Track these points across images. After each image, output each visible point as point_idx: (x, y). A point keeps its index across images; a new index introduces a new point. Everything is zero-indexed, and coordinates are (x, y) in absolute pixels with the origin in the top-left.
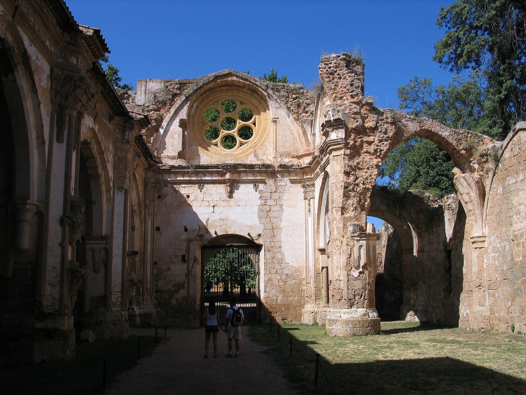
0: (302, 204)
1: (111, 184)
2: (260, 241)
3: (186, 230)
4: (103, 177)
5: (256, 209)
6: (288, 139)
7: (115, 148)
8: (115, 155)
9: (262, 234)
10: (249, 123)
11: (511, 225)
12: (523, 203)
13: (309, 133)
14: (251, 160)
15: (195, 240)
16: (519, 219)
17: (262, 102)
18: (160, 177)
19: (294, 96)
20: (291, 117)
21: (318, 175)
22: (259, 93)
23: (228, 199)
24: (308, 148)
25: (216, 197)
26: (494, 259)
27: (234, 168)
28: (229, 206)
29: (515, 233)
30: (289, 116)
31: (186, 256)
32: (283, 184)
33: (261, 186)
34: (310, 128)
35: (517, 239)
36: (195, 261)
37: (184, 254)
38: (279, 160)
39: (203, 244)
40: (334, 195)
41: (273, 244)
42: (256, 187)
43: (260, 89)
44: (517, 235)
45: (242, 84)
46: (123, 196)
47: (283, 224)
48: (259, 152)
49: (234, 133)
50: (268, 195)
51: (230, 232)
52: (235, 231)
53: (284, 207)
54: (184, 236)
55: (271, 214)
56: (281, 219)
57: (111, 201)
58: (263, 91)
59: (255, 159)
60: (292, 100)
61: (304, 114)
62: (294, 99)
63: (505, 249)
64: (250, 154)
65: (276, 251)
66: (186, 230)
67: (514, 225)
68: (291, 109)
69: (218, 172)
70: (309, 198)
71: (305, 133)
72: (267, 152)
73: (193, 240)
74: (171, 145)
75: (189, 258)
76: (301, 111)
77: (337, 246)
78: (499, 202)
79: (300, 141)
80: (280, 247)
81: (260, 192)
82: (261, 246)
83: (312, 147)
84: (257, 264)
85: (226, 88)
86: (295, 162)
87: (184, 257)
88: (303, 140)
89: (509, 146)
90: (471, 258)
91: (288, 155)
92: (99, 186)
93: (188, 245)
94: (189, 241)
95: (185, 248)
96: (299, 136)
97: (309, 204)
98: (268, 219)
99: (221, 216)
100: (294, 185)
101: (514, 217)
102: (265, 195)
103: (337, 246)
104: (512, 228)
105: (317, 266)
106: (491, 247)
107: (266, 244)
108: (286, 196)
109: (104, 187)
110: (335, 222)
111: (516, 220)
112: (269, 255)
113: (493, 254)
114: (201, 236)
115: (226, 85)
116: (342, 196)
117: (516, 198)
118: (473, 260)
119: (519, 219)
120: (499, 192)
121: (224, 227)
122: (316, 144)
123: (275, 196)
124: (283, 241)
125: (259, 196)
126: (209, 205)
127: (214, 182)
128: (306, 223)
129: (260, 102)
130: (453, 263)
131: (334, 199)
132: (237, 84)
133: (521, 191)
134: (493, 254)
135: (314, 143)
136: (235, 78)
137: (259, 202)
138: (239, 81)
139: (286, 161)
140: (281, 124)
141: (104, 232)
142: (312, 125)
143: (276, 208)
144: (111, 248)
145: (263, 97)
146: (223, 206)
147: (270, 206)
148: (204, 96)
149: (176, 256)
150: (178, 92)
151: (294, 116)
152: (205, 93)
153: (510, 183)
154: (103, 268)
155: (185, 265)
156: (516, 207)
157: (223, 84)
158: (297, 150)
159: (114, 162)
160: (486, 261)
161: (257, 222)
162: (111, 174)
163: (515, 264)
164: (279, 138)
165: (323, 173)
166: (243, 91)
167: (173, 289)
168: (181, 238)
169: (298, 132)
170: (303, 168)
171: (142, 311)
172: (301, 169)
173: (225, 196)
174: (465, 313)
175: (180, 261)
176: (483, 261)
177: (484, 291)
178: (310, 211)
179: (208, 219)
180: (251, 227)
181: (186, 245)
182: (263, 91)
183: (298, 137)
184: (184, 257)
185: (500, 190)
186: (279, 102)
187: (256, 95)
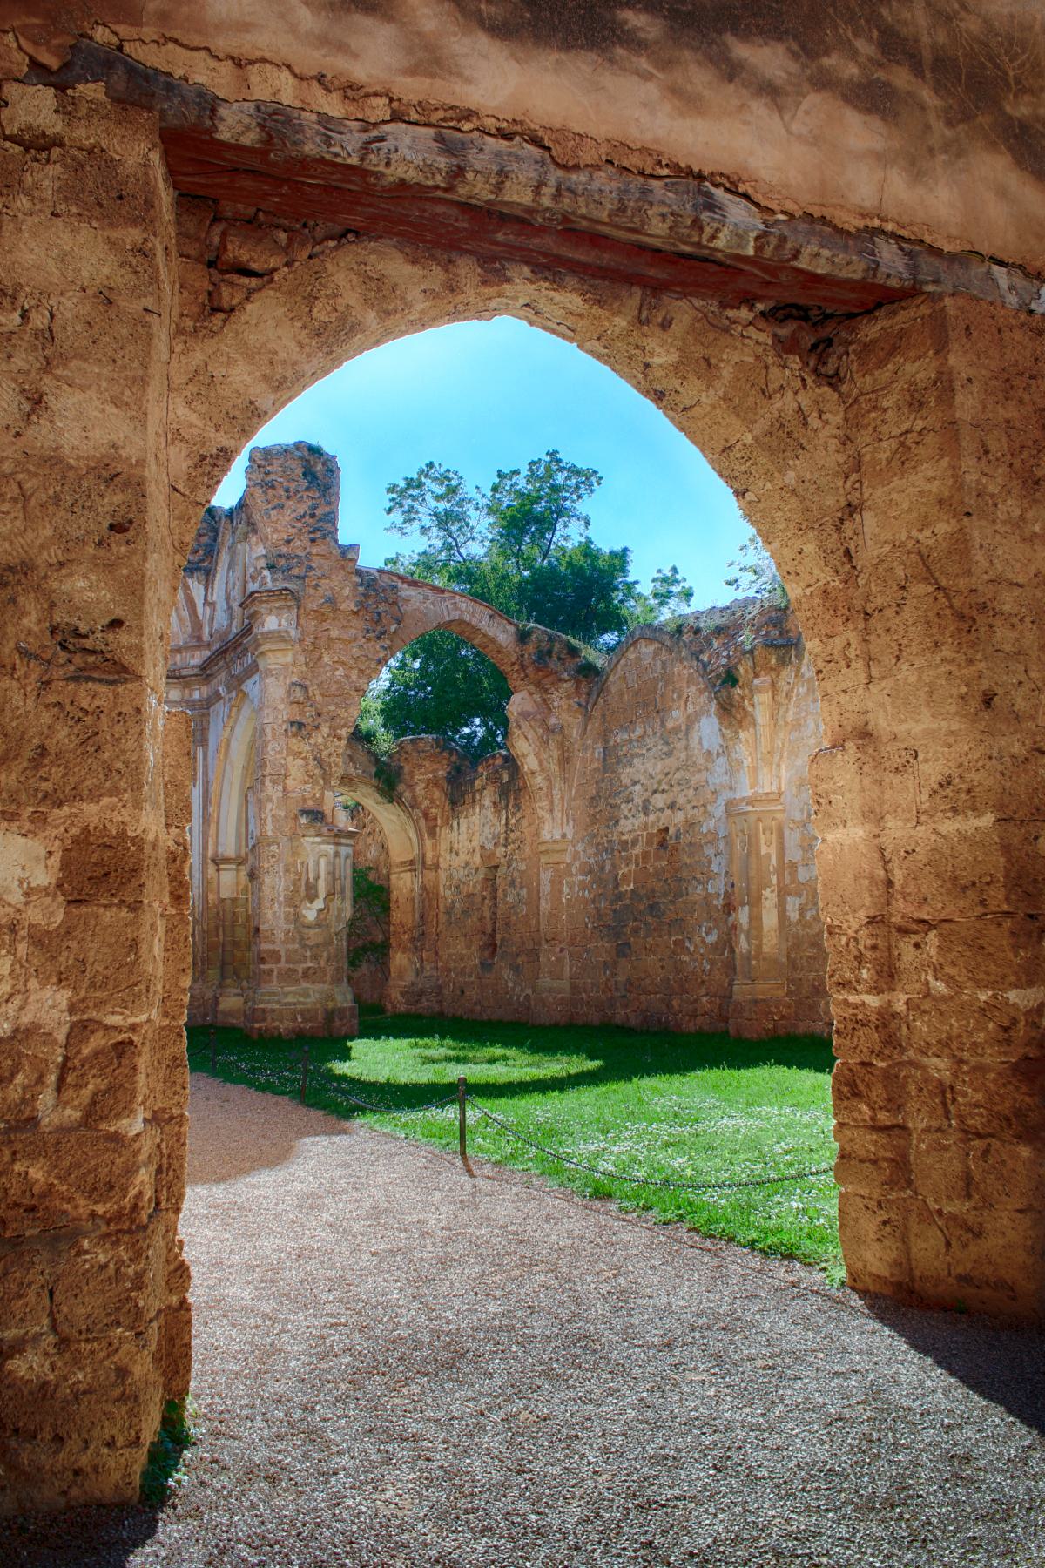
11: (617, 822)
13: (199, 602)
16: (630, 810)
26: (583, 887)
29: (624, 838)
34: (202, 587)
35: (625, 850)
44: (626, 842)
63: (602, 869)
67: (622, 822)
77: (273, 856)
83: (206, 630)
89: (619, 667)
90: (538, 885)
101: (623, 806)
104: (619, 828)
105: (211, 897)
106: (577, 864)
110: (269, 806)
111: (626, 813)
113: (581, 878)
118: (542, 887)
122: (216, 626)
130: (500, 893)
134: (581, 878)
156: (627, 787)
160: (566, 890)
163: (620, 896)
174: (523, 994)
176: (561, 892)
177: (562, 950)
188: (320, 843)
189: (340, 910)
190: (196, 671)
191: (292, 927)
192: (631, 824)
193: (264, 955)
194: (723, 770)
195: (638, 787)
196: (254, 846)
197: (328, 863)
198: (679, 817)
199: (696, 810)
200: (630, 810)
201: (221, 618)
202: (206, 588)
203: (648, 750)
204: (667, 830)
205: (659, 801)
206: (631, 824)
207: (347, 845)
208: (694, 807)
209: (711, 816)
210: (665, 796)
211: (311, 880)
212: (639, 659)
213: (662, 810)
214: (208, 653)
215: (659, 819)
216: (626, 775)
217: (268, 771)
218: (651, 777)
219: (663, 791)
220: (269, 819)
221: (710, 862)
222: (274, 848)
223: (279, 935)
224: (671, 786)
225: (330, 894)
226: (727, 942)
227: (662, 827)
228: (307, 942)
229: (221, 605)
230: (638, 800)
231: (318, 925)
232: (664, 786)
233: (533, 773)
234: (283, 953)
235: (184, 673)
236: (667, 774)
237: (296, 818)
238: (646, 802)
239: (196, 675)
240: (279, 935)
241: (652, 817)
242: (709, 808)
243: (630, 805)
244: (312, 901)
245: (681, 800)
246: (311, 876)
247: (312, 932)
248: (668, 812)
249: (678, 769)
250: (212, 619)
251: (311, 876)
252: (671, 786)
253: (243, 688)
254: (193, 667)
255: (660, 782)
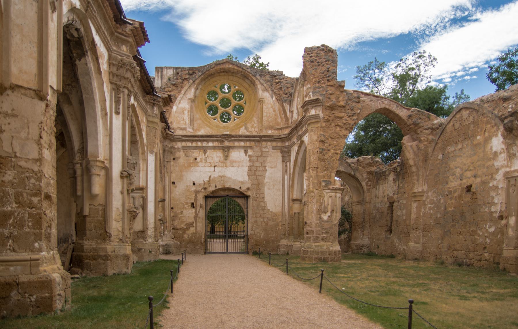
0: (280, 166)
1: (146, 148)
2: (249, 193)
3: (194, 184)
4: (139, 142)
5: (246, 169)
6: (271, 115)
7: (148, 121)
8: (147, 126)
9: (251, 188)
10: (242, 102)
12: (458, 167)
13: (288, 111)
14: (242, 131)
15: (201, 192)
17: (252, 86)
18: (174, 143)
19: (277, 81)
20: (274, 98)
21: (294, 144)
22: (250, 78)
23: (225, 161)
24: (286, 123)
25: (216, 159)
27: (229, 137)
28: (226, 167)
30: (272, 97)
31: (194, 204)
32: (267, 150)
33: (250, 152)
34: (288, 106)
36: (201, 207)
37: (193, 201)
38: (264, 131)
39: (206, 194)
40: (311, 158)
41: (258, 195)
42: (246, 152)
43: (250, 75)
45: (236, 71)
46: (154, 158)
47: (266, 180)
48: (249, 125)
49: (229, 111)
50: (254, 158)
51: (227, 186)
52: (230, 185)
53: (267, 168)
54: (193, 189)
55: (257, 173)
56: (265, 177)
57: (146, 160)
58: (252, 77)
59: (245, 131)
60: (275, 84)
61: (284, 96)
62: (277, 83)
64: (241, 127)
65: (260, 200)
66: (194, 184)
68: (275, 91)
69: (218, 141)
70: (286, 161)
71: (285, 111)
72: (255, 125)
73: (199, 192)
74: (182, 119)
75: (196, 204)
76: (281, 93)
77: (312, 197)
78: (439, 165)
79: (280, 117)
80: (263, 198)
81: (250, 156)
82: (250, 196)
83: (290, 121)
84: (246, 210)
85: (223, 74)
86: (276, 133)
87: (193, 204)
88: (283, 116)
91: (271, 128)
92: (138, 150)
93: (196, 195)
94: (197, 192)
95: (193, 198)
96: (280, 113)
97: (286, 166)
98: (255, 177)
99: (220, 174)
100: (275, 151)
101: (450, 177)
102: (253, 158)
103: (312, 197)
107: (253, 195)
108: (269, 158)
109: (140, 150)
110: (311, 179)
111: (452, 179)
112: (255, 204)
114: (205, 189)
115: (223, 72)
116: (317, 159)
117: (453, 163)
119: (454, 179)
120: (439, 158)
121: (222, 182)
122: (293, 119)
123: (260, 159)
124: (266, 193)
125: (248, 159)
126: (211, 166)
127: (214, 148)
128: (283, 180)
129: (249, 85)
131: (311, 161)
132: (232, 70)
133: (458, 157)
135: (292, 119)
136: (231, 66)
137: (248, 164)
138: (234, 69)
139: (270, 132)
140: (266, 103)
141: (142, 184)
142: (290, 104)
143: (261, 169)
144: (147, 195)
145: (253, 82)
146: (222, 167)
147: (257, 167)
148: (206, 80)
149: (187, 203)
150: (187, 77)
151: (277, 97)
152: (207, 78)
153: (450, 151)
154: (141, 211)
155: (194, 210)
156: (452, 169)
157: (221, 71)
158: (278, 124)
159: (147, 131)
161: (246, 178)
162: (145, 141)
164: (265, 114)
165: (299, 142)
166: (237, 77)
167: (185, 227)
168: (191, 190)
169: (279, 110)
170: (282, 138)
171: (164, 243)
172: (280, 138)
173: (222, 159)
175: (190, 207)
178: (286, 171)
179: (210, 176)
180: (242, 183)
181: (194, 195)
182: (252, 77)
183: (279, 114)
184: (193, 204)
185: (440, 157)
186: (265, 85)
187: (247, 80)
188: (329, 192)
189: (336, 216)
190: (287, 135)
191: (318, 222)
192: (454, 184)
193: (308, 232)
194: (503, 159)
195: (458, 169)
196: (305, 194)
197: (332, 200)
198: (478, 180)
199: (487, 177)
200: (454, 179)
201: (295, 116)
202: (290, 106)
203: (464, 154)
204: (471, 186)
205: (469, 174)
206: (454, 184)
207: (339, 193)
208: (486, 176)
209: (495, 179)
210: (471, 172)
211: (326, 205)
212: (461, 117)
213: (469, 178)
214: (291, 129)
215: (467, 182)
216: (452, 164)
217: (311, 166)
218: (465, 165)
219: (470, 170)
220: (311, 184)
221: (493, 198)
222: (312, 194)
223: (314, 224)
224: (475, 168)
225: (332, 211)
226: (502, 231)
227: (468, 184)
228: (324, 227)
229: (295, 111)
230: (458, 174)
231: (327, 221)
232: (471, 168)
233: (411, 166)
234: (315, 231)
235: (283, 136)
236: (473, 163)
237: (320, 183)
238: (462, 175)
239: (286, 137)
240: (314, 224)
241: (464, 181)
242: (494, 175)
243: (454, 177)
244: (325, 213)
245: (480, 173)
246: (326, 204)
247: (326, 224)
248: (473, 179)
249: (478, 161)
250: (292, 116)
251: (326, 204)
252: (475, 168)
253: (303, 139)
254: (285, 134)
255: (469, 167)
